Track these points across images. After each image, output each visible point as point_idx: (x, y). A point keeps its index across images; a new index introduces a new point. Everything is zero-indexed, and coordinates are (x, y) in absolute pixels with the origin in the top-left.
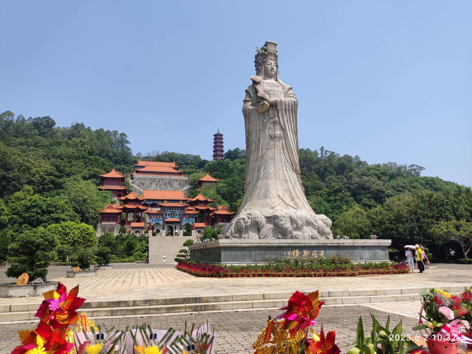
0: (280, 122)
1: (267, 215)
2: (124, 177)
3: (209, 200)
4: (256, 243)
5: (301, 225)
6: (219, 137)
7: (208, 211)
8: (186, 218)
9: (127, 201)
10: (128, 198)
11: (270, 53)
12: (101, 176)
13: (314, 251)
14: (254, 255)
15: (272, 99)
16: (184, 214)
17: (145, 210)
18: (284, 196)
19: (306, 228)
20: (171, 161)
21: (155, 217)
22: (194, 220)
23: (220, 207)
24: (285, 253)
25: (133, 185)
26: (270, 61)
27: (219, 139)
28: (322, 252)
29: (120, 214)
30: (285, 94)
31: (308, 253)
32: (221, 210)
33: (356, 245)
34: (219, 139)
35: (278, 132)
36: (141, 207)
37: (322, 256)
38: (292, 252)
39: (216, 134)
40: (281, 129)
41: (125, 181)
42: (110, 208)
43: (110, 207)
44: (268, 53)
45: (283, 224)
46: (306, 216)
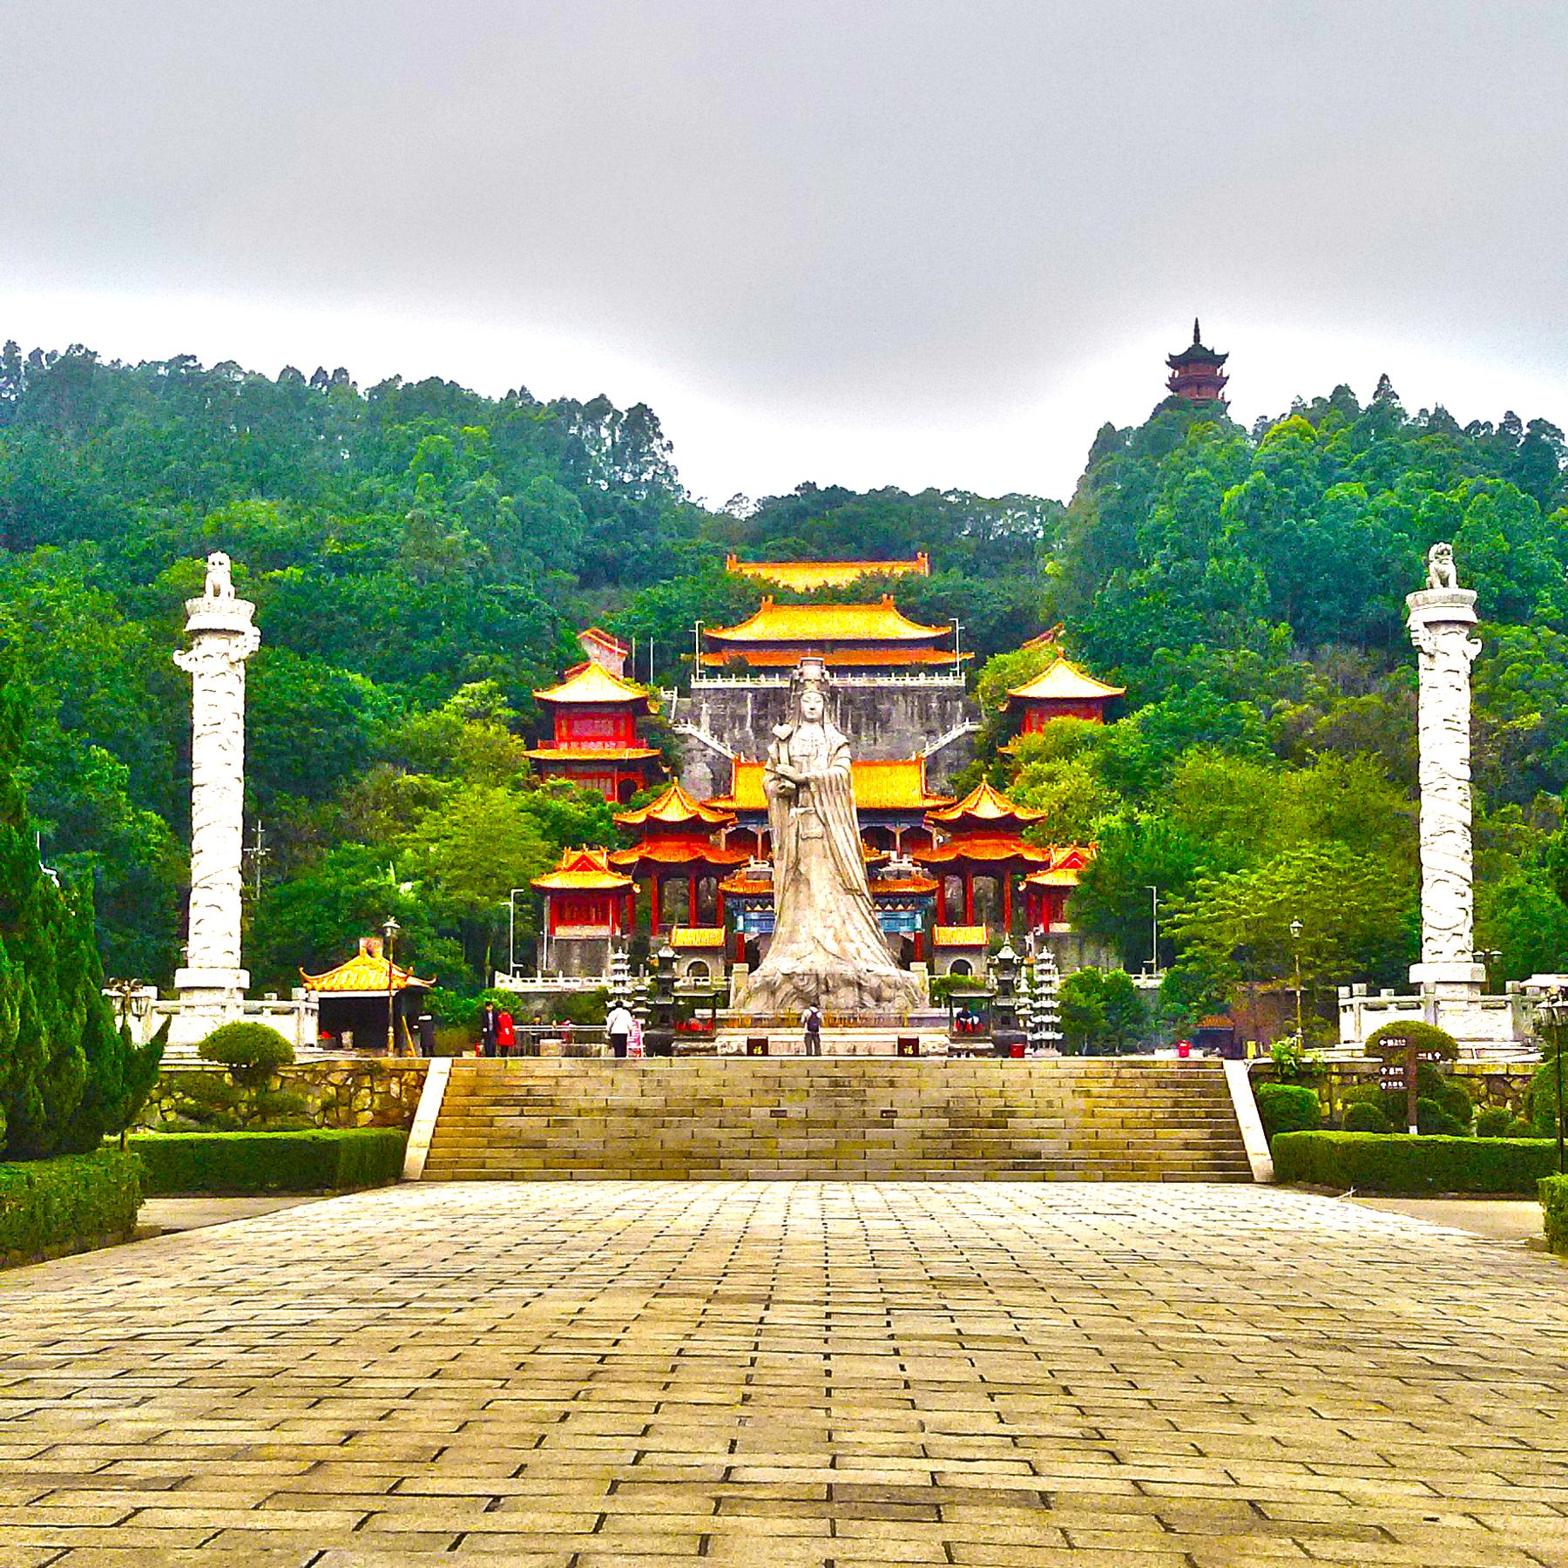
2: (645, 699)
3: (1022, 814)
7: (1020, 866)
9: (656, 830)
10: (656, 816)
12: (540, 699)
15: (801, 777)
17: (737, 865)
19: (842, 992)
21: (758, 908)
22: (918, 917)
23: (1059, 856)
25: (690, 729)
32: (1061, 867)
35: (817, 829)
39: (1178, 352)
41: (649, 713)
42: (584, 868)
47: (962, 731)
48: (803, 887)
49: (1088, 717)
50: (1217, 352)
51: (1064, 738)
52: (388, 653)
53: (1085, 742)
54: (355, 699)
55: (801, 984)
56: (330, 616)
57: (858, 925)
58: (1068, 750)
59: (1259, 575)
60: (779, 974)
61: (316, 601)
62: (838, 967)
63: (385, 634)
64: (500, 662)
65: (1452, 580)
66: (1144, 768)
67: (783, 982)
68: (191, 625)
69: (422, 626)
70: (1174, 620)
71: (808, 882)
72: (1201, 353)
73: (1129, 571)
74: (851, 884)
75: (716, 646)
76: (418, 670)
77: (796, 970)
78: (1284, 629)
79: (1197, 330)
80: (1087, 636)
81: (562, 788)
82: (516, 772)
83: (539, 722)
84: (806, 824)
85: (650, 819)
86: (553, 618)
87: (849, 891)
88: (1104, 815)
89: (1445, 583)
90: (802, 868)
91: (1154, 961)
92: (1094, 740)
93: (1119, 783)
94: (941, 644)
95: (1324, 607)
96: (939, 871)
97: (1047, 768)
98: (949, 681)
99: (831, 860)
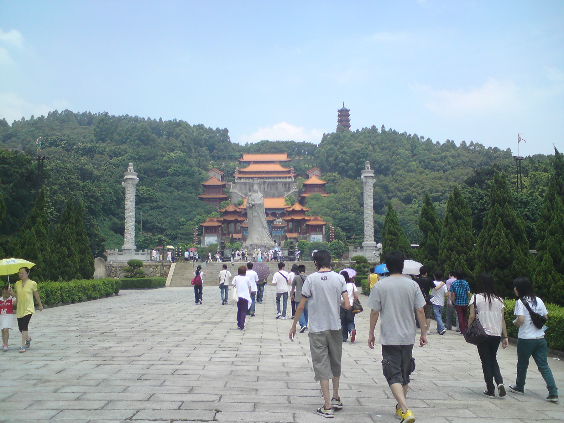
3: (304, 210)
6: (344, 113)
7: (304, 220)
8: (275, 230)
9: (227, 213)
10: (227, 210)
15: (253, 203)
16: (273, 227)
17: (244, 220)
20: (281, 152)
23: (312, 218)
27: (344, 116)
29: (220, 226)
34: (344, 116)
35: (256, 215)
36: (239, 219)
39: (340, 109)
43: (211, 221)
47: (293, 191)
50: (348, 109)
65: (370, 168)
68: (126, 177)
72: (344, 109)
75: (241, 172)
85: (225, 210)
87: (263, 227)
89: (368, 169)
94: (289, 172)
96: (288, 221)
98: (290, 180)
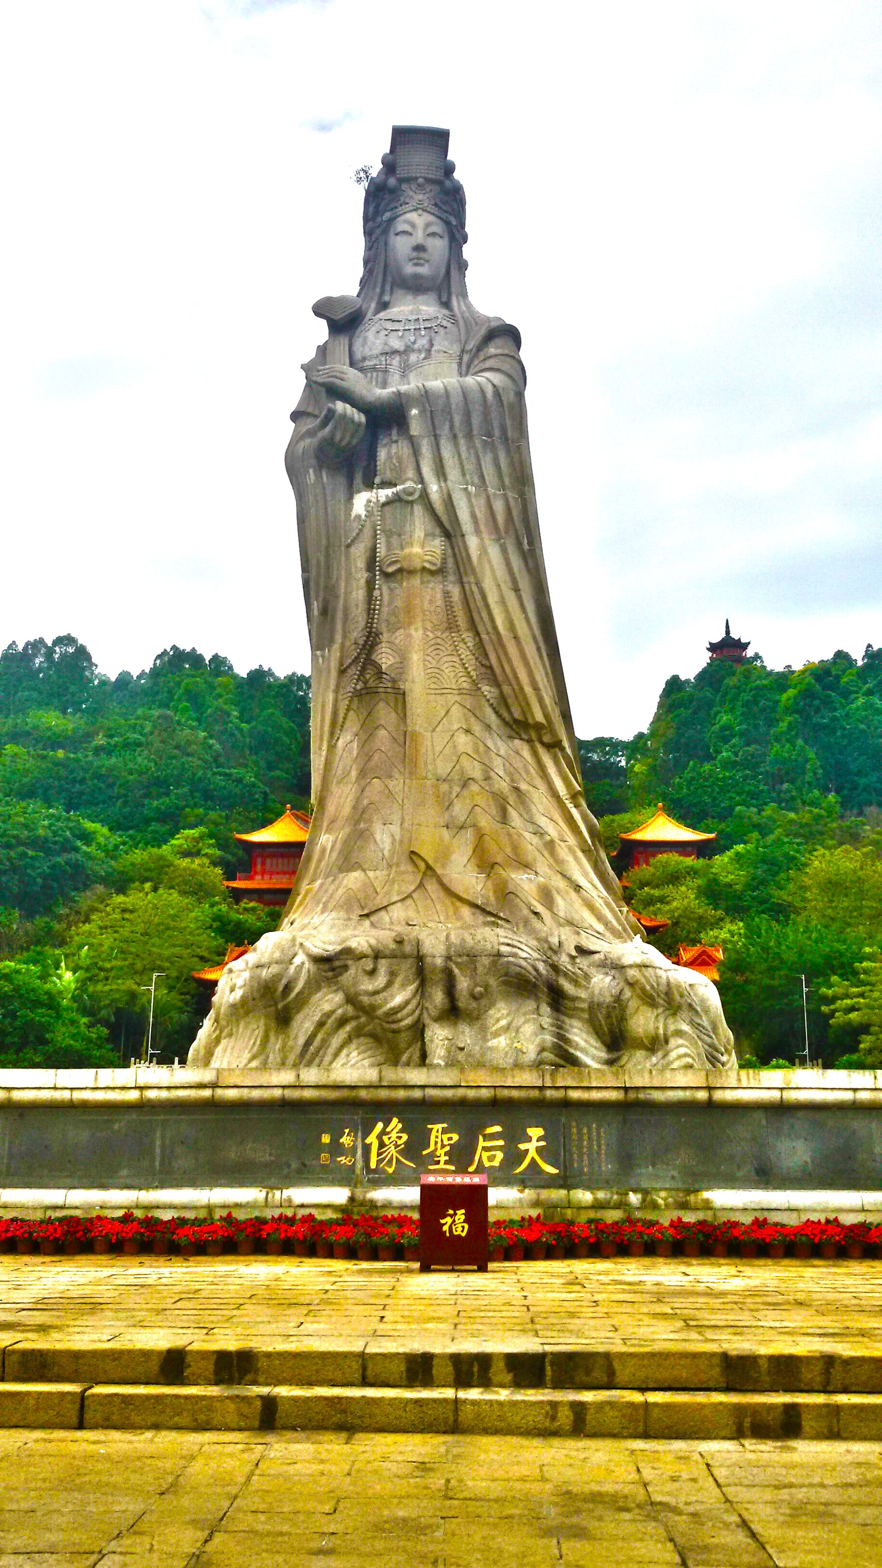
0: (425, 495)
1: (317, 951)
4: (169, 1088)
5: (474, 997)
11: (409, 180)
13: (490, 1130)
14: (163, 1146)
18: (445, 855)
24: (326, 1139)
26: (413, 216)
28: (535, 1132)
30: (466, 358)
31: (455, 1137)
33: (792, 1096)
37: (532, 1154)
38: (366, 1134)
40: (438, 531)
44: (401, 181)
45: (376, 993)
46: (504, 949)
48: (385, 714)
49: (688, 855)
50: (743, 641)
51: (670, 869)
52: (127, 810)
53: (688, 873)
54: (87, 837)
55: (368, 985)
56: (83, 781)
57: (543, 822)
58: (675, 878)
59: (811, 755)
60: (300, 958)
61: (72, 771)
62: (487, 932)
63: (125, 796)
64: (213, 815)
66: (743, 892)
67: (314, 985)
69: (154, 790)
70: (747, 788)
71: (400, 698)
73: (701, 764)
74: (526, 707)
76: (147, 821)
77: (353, 944)
78: (832, 797)
79: (727, 627)
80: (679, 800)
81: (253, 909)
82: (214, 896)
83: (240, 861)
84: (397, 534)
86: (265, 793)
88: (712, 930)
90: (385, 658)
91: (806, 1052)
92: (696, 872)
93: (722, 903)
95: (863, 781)
97: (657, 893)
99: (468, 636)
